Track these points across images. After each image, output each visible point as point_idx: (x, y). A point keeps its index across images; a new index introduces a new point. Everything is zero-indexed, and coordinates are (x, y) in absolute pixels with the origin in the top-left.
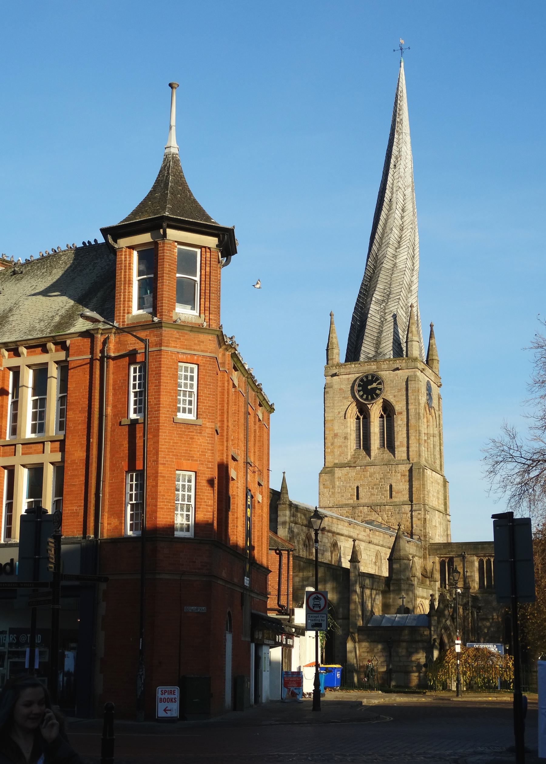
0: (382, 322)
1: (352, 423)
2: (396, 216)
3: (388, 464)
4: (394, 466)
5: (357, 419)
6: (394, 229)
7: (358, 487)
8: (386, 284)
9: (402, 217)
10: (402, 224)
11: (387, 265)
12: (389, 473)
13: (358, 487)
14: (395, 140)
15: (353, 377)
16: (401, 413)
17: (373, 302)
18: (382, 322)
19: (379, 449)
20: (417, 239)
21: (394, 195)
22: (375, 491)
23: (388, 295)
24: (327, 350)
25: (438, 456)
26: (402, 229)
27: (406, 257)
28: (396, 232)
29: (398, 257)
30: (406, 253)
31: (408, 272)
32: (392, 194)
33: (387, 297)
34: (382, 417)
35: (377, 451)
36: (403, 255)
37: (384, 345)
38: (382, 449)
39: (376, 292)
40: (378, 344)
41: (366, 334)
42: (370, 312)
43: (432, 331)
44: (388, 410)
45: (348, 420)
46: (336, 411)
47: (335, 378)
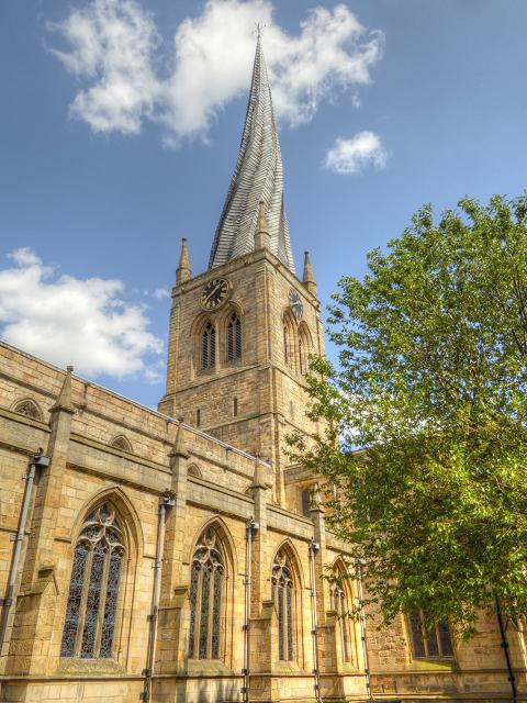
13: (199, 411)
33: (243, 211)
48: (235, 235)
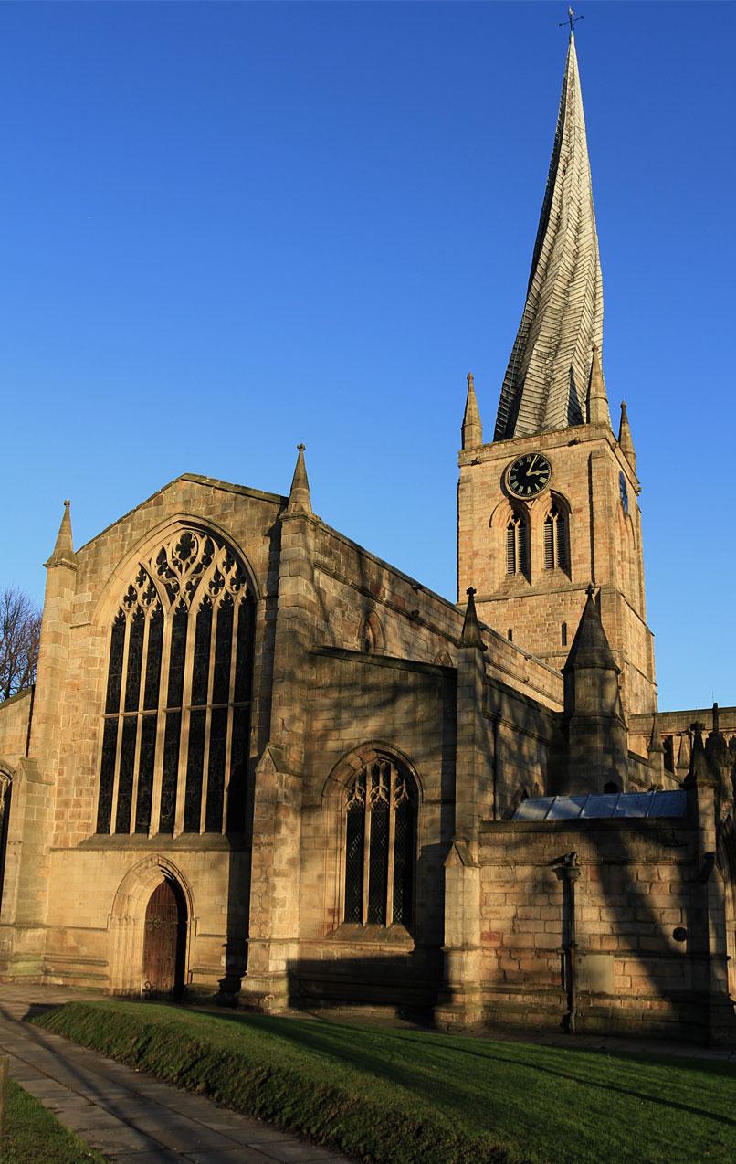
0: (549, 382)
1: (501, 535)
2: (568, 238)
3: (561, 590)
4: (569, 593)
5: (509, 529)
6: (564, 255)
7: (510, 631)
8: (553, 331)
9: (577, 240)
10: (578, 248)
11: (555, 304)
12: (560, 605)
13: (510, 631)
14: (564, 137)
15: (502, 463)
16: (580, 510)
17: (533, 357)
18: (549, 382)
19: (544, 571)
20: (599, 273)
21: (564, 210)
22: (539, 636)
23: (557, 346)
24: (463, 429)
25: (637, 594)
26: (576, 256)
27: (584, 293)
28: (569, 260)
29: (571, 294)
30: (584, 288)
31: (586, 314)
32: (561, 210)
33: (555, 349)
34: (549, 521)
35: (541, 574)
36: (580, 291)
37: (552, 414)
38: (549, 571)
39: (538, 343)
40: (542, 413)
41: (523, 402)
42: (530, 370)
43: (623, 414)
44: (560, 507)
45: (495, 528)
46: (477, 517)
47: (475, 467)
48: (548, 384)
